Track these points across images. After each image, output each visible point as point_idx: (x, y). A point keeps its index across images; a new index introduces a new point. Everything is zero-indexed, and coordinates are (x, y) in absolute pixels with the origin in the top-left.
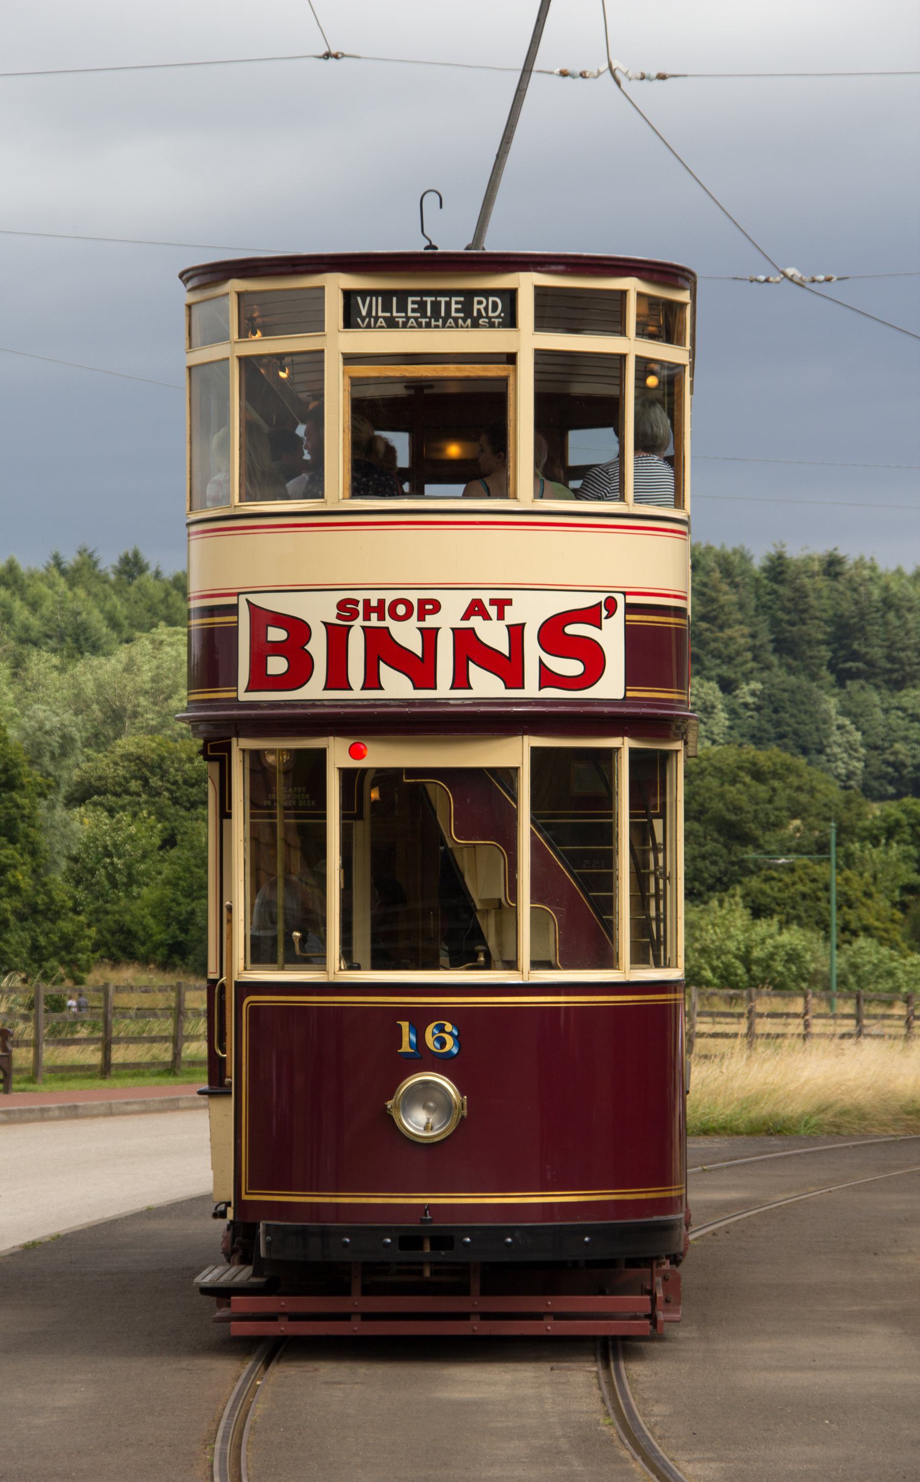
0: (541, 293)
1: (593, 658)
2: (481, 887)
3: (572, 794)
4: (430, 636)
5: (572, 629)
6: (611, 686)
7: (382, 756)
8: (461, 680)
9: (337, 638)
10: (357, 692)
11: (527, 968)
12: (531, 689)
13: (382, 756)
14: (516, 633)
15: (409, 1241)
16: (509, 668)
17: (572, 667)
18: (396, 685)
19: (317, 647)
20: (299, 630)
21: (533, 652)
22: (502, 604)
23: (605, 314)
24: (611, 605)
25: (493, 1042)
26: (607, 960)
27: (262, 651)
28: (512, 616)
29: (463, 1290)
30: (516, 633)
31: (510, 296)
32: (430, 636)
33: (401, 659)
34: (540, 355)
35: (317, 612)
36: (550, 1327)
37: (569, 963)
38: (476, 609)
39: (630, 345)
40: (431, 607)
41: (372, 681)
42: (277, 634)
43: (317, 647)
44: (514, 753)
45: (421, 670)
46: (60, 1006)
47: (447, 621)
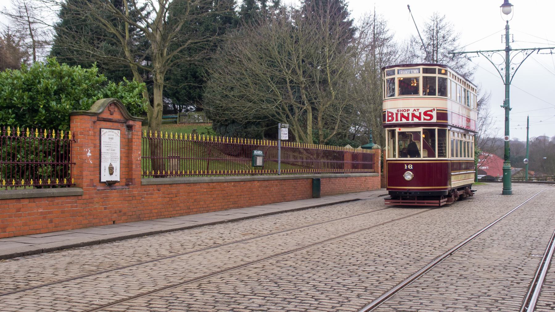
0: (423, 69)
1: (431, 117)
2: (419, 148)
3: (430, 134)
4: (408, 114)
5: (428, 113)
6: (434, 120)
7: (403, 130)
8: (413, 120)
9: (397, 114)
10: (399, 122)
11: (423, 157)
12: (422, 121)
13: (403, 130)
14: (420, 113)
15: (406, 193)
16: (419, 118)
17: (429, 118)
18: (404, 121)
19: (395, 116)
20: (392, 114)
21: (423, 116)
22: (418, 110)
23: (433, 71)
24: (434, 110)
25: (417, 168)
26: (435, 157)
27: (388, 116)
28: (419, 111)
29: (414, 200)
30: (420, 113)
31: (419, 69)
32: (408, 114)
33: (405, 117)
34: (423, 77)
35: (394, 111)
36: (426, 204)
37: (429, 157)
38: (415, 110)
39: (437, 75)
40: (408, 110)
41: (401, 120)
42: (390, 114)
43: (395, 116)
44: (420, 129)
45: (407, 119)
46: (467, 193)
47: (411, 112)
